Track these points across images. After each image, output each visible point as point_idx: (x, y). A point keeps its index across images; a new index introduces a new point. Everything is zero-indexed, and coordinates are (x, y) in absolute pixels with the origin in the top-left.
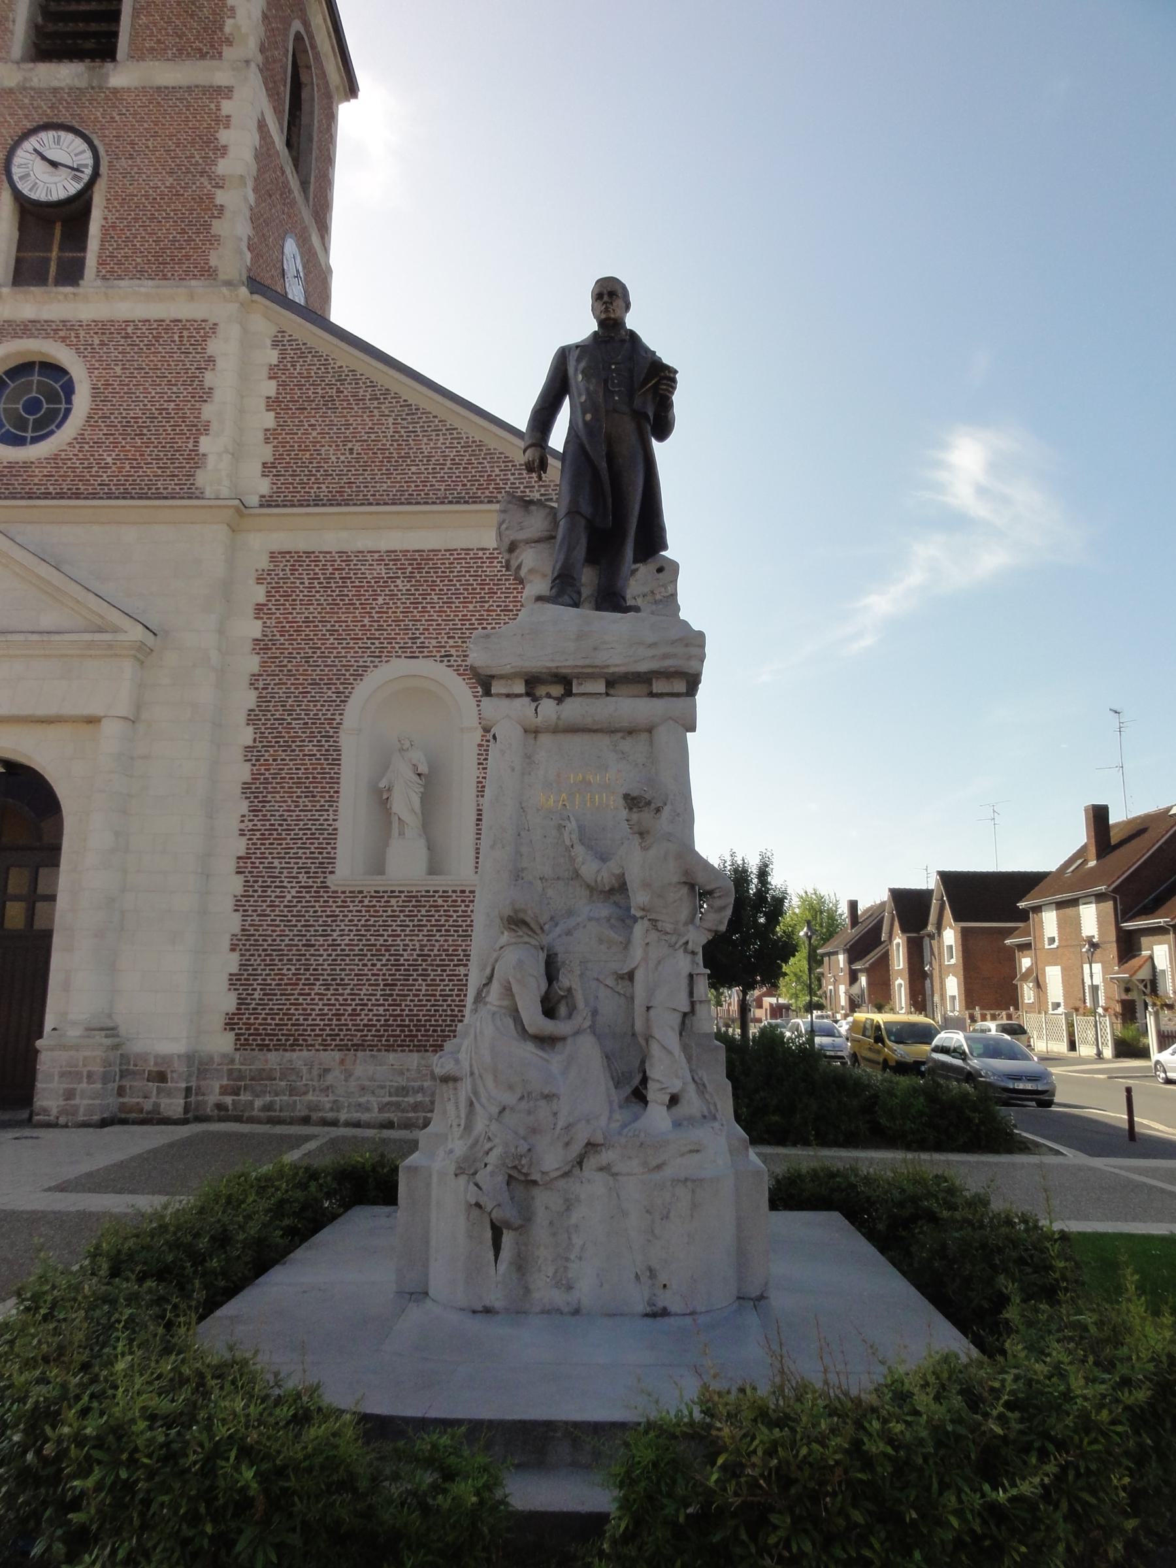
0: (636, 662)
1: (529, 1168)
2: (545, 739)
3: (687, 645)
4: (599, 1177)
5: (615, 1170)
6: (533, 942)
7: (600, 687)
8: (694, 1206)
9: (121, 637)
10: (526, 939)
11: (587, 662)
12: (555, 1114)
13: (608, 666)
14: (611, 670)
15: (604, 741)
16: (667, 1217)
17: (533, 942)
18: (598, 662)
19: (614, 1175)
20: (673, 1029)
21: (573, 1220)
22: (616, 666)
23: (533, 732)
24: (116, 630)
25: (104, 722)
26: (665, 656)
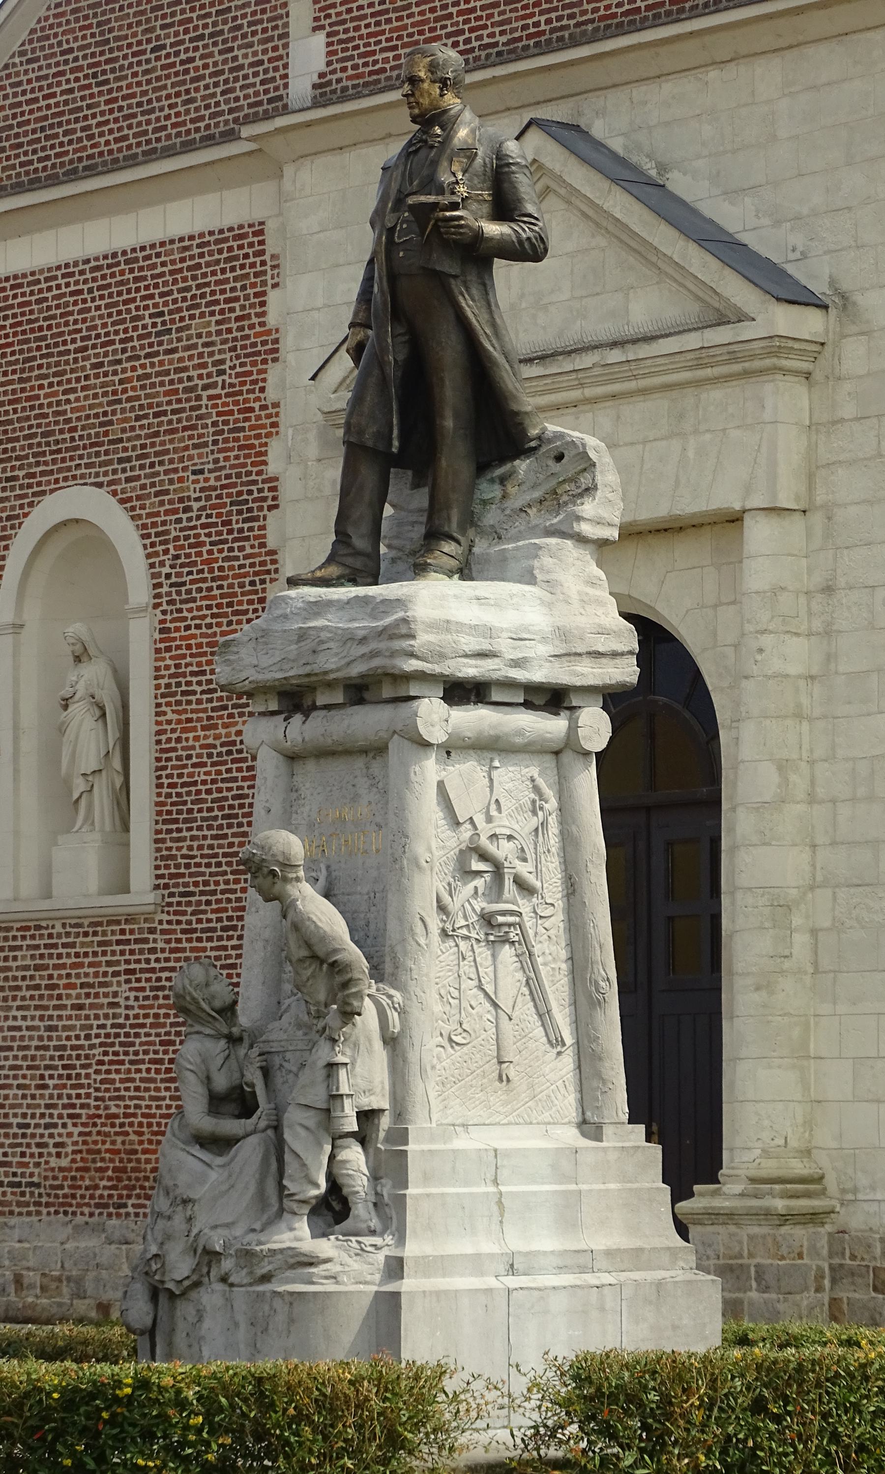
0: (348, 664)
1: (163, 1274)
2: (311, 766)
3: (392, 637)
4: (219, 1287)
5: (232, 1280)
6: (208, 1031)
7: (338, 697)
8: (291, 1321)
9: (747, 332)
10: (198, 1028)
11: (307, 669)
12: (190, 1219)
13: (326, 673)
14: (332, 676)
15: (359, 763)
16: (266, 1329)
17: (208, 1031)
18: (316, 669)
19: (232, 1285)
20: (307, 1128)
21: (203, 1332)
22: (332, 671)
23: (293, 758)
24: (742, 317)
25: (748, 520)
26: (374, 654)
